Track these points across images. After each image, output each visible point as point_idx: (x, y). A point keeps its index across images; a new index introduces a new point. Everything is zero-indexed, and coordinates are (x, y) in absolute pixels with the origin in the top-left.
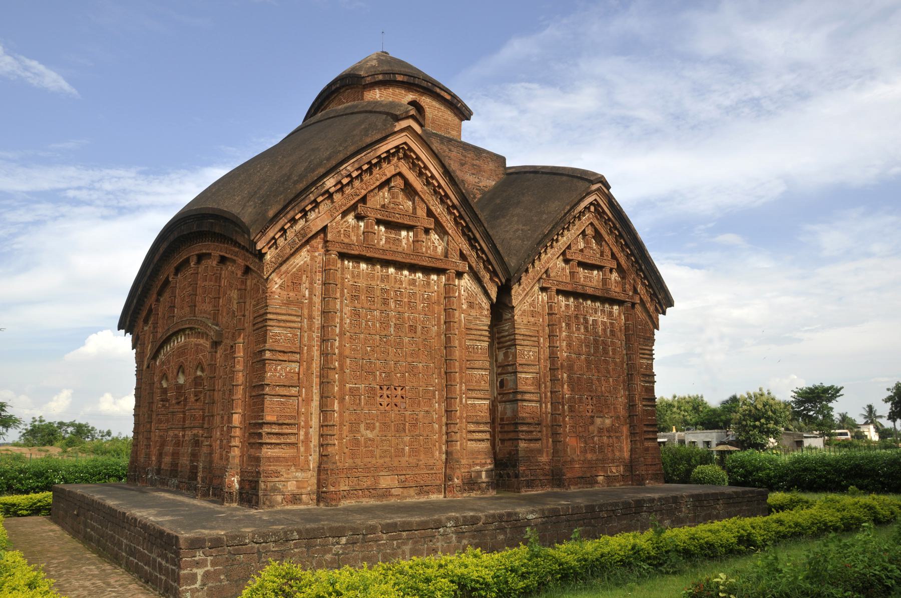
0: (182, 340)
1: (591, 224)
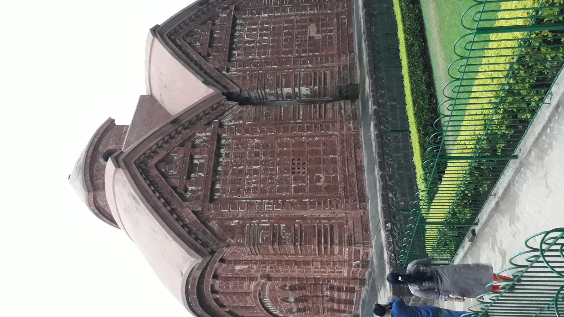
0: (267, 300)
1: (183, 38)
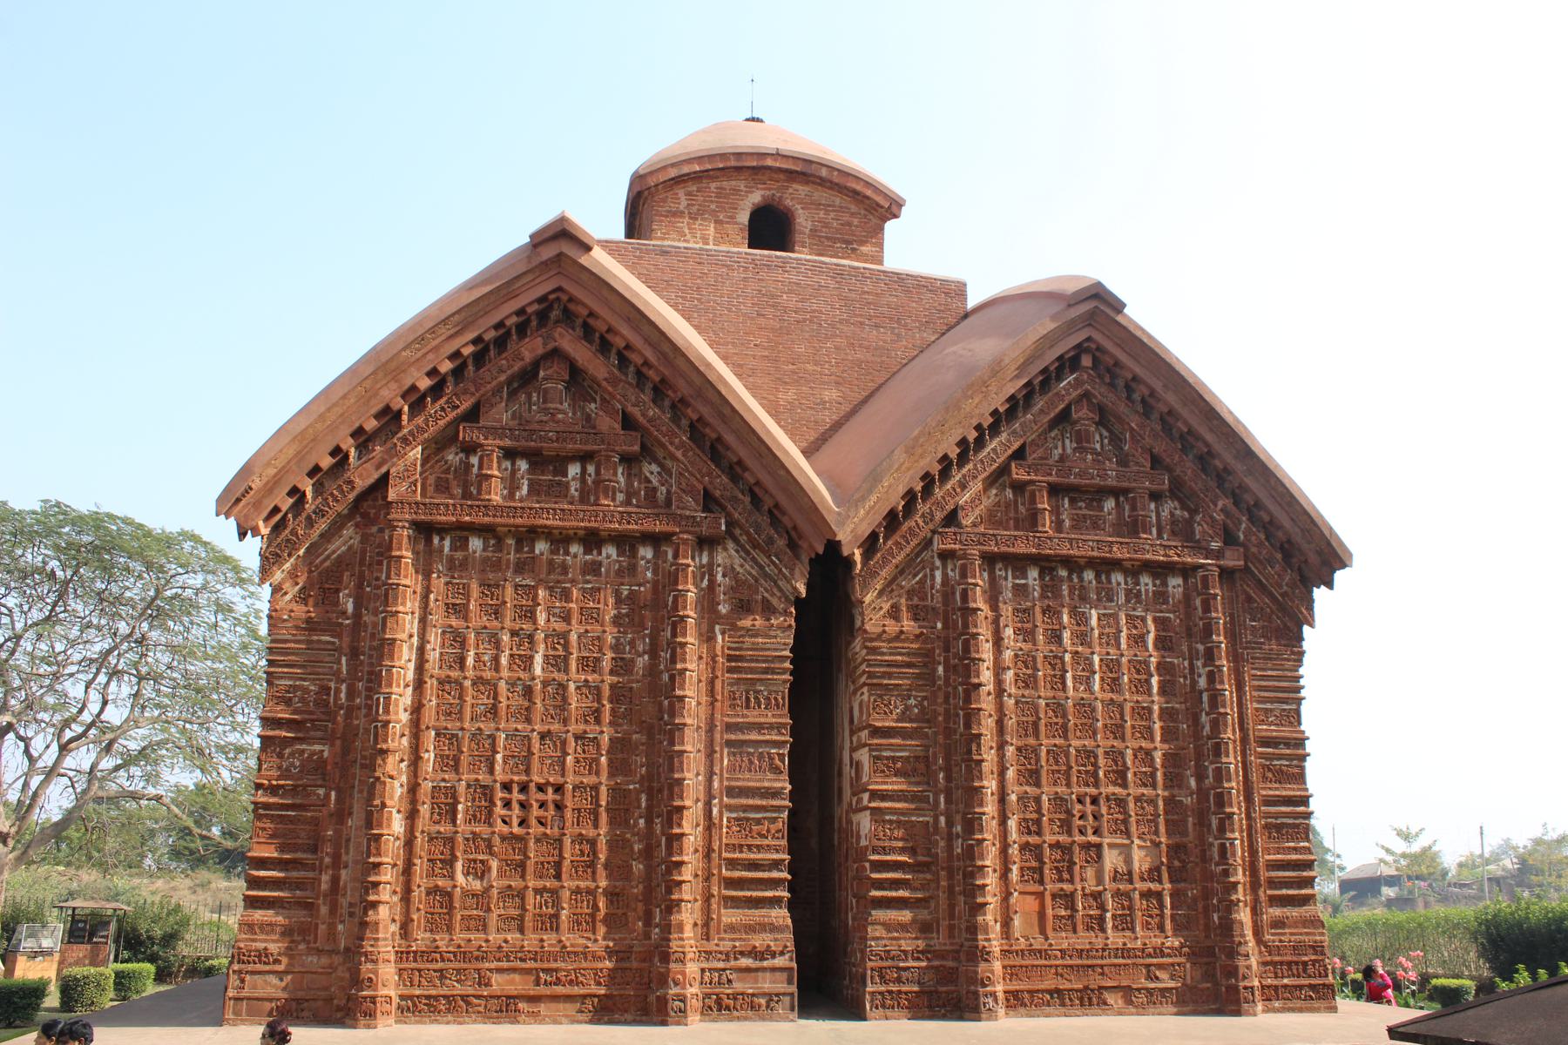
1: (1086, 395)
